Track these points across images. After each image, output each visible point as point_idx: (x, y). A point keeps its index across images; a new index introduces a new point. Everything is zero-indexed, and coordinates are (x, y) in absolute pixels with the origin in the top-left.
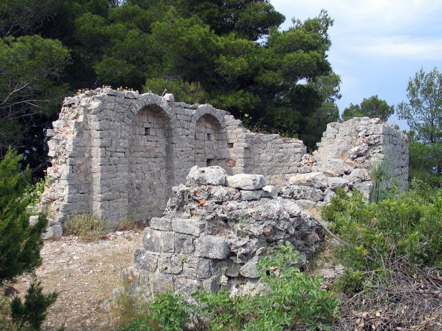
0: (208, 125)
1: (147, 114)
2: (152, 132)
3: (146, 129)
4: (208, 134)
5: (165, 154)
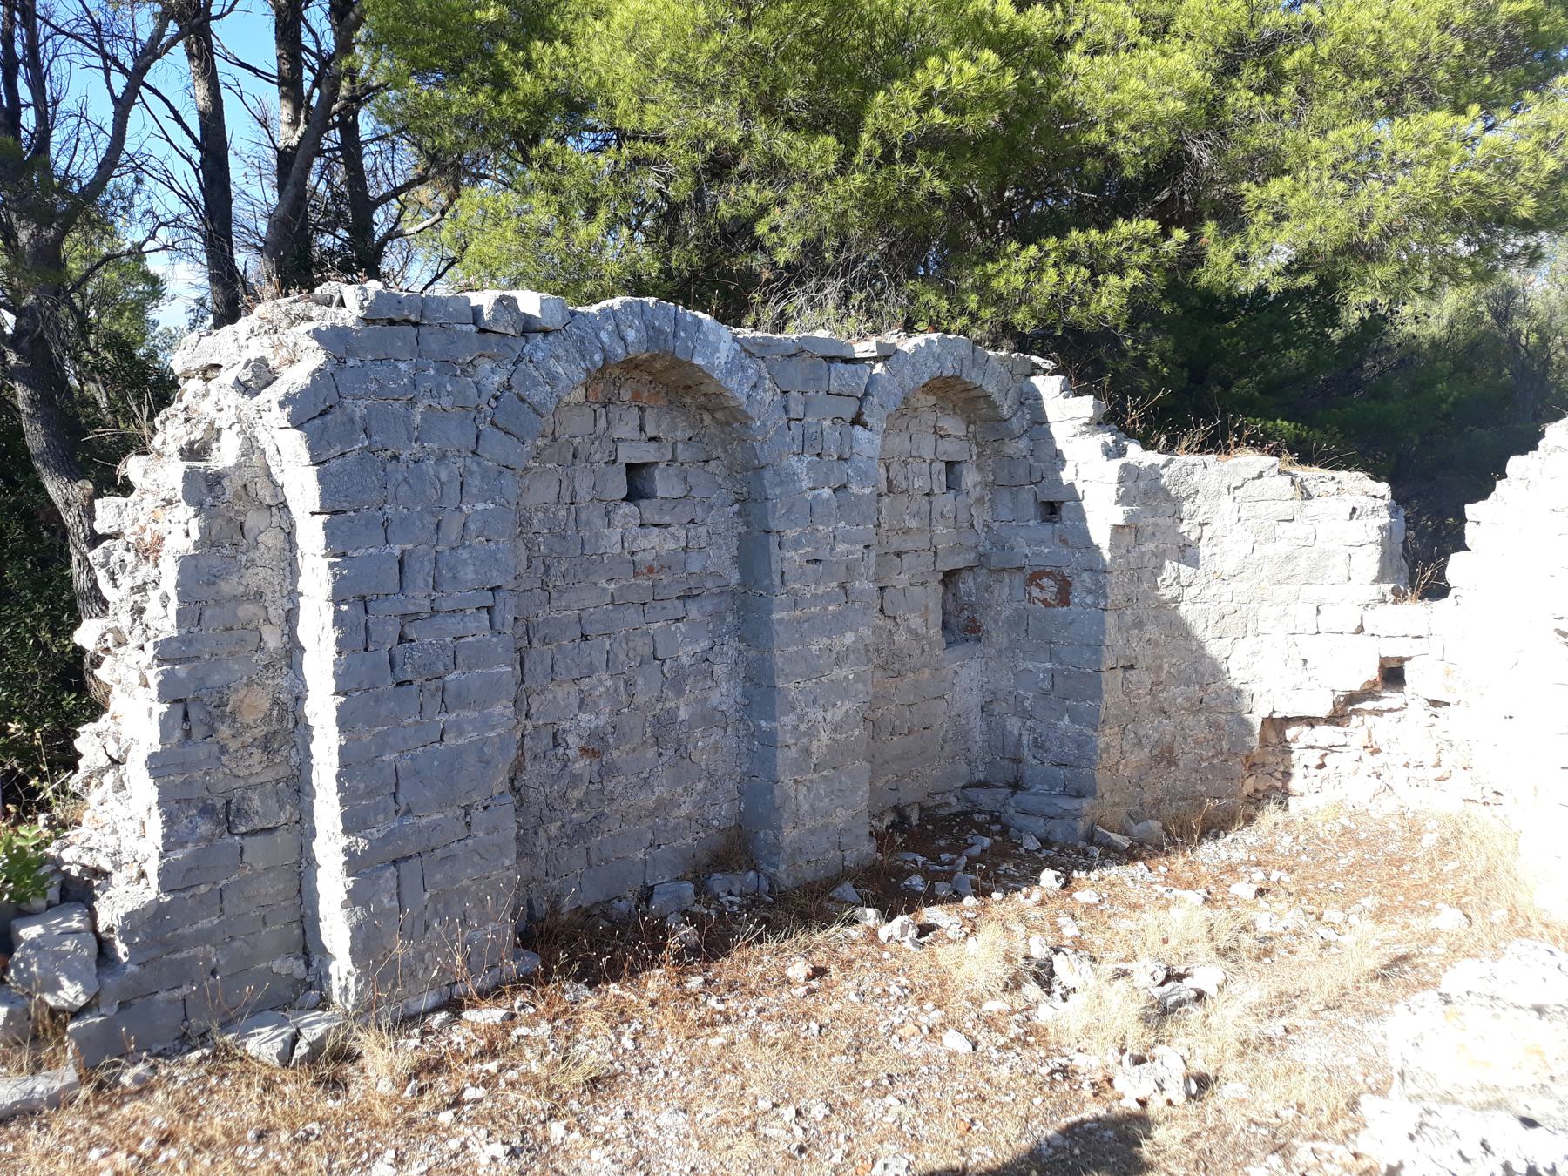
0: (953, 425)
1: (636, 396)
2: (665, 485)
3: (634, 470)
5: (734, 577)
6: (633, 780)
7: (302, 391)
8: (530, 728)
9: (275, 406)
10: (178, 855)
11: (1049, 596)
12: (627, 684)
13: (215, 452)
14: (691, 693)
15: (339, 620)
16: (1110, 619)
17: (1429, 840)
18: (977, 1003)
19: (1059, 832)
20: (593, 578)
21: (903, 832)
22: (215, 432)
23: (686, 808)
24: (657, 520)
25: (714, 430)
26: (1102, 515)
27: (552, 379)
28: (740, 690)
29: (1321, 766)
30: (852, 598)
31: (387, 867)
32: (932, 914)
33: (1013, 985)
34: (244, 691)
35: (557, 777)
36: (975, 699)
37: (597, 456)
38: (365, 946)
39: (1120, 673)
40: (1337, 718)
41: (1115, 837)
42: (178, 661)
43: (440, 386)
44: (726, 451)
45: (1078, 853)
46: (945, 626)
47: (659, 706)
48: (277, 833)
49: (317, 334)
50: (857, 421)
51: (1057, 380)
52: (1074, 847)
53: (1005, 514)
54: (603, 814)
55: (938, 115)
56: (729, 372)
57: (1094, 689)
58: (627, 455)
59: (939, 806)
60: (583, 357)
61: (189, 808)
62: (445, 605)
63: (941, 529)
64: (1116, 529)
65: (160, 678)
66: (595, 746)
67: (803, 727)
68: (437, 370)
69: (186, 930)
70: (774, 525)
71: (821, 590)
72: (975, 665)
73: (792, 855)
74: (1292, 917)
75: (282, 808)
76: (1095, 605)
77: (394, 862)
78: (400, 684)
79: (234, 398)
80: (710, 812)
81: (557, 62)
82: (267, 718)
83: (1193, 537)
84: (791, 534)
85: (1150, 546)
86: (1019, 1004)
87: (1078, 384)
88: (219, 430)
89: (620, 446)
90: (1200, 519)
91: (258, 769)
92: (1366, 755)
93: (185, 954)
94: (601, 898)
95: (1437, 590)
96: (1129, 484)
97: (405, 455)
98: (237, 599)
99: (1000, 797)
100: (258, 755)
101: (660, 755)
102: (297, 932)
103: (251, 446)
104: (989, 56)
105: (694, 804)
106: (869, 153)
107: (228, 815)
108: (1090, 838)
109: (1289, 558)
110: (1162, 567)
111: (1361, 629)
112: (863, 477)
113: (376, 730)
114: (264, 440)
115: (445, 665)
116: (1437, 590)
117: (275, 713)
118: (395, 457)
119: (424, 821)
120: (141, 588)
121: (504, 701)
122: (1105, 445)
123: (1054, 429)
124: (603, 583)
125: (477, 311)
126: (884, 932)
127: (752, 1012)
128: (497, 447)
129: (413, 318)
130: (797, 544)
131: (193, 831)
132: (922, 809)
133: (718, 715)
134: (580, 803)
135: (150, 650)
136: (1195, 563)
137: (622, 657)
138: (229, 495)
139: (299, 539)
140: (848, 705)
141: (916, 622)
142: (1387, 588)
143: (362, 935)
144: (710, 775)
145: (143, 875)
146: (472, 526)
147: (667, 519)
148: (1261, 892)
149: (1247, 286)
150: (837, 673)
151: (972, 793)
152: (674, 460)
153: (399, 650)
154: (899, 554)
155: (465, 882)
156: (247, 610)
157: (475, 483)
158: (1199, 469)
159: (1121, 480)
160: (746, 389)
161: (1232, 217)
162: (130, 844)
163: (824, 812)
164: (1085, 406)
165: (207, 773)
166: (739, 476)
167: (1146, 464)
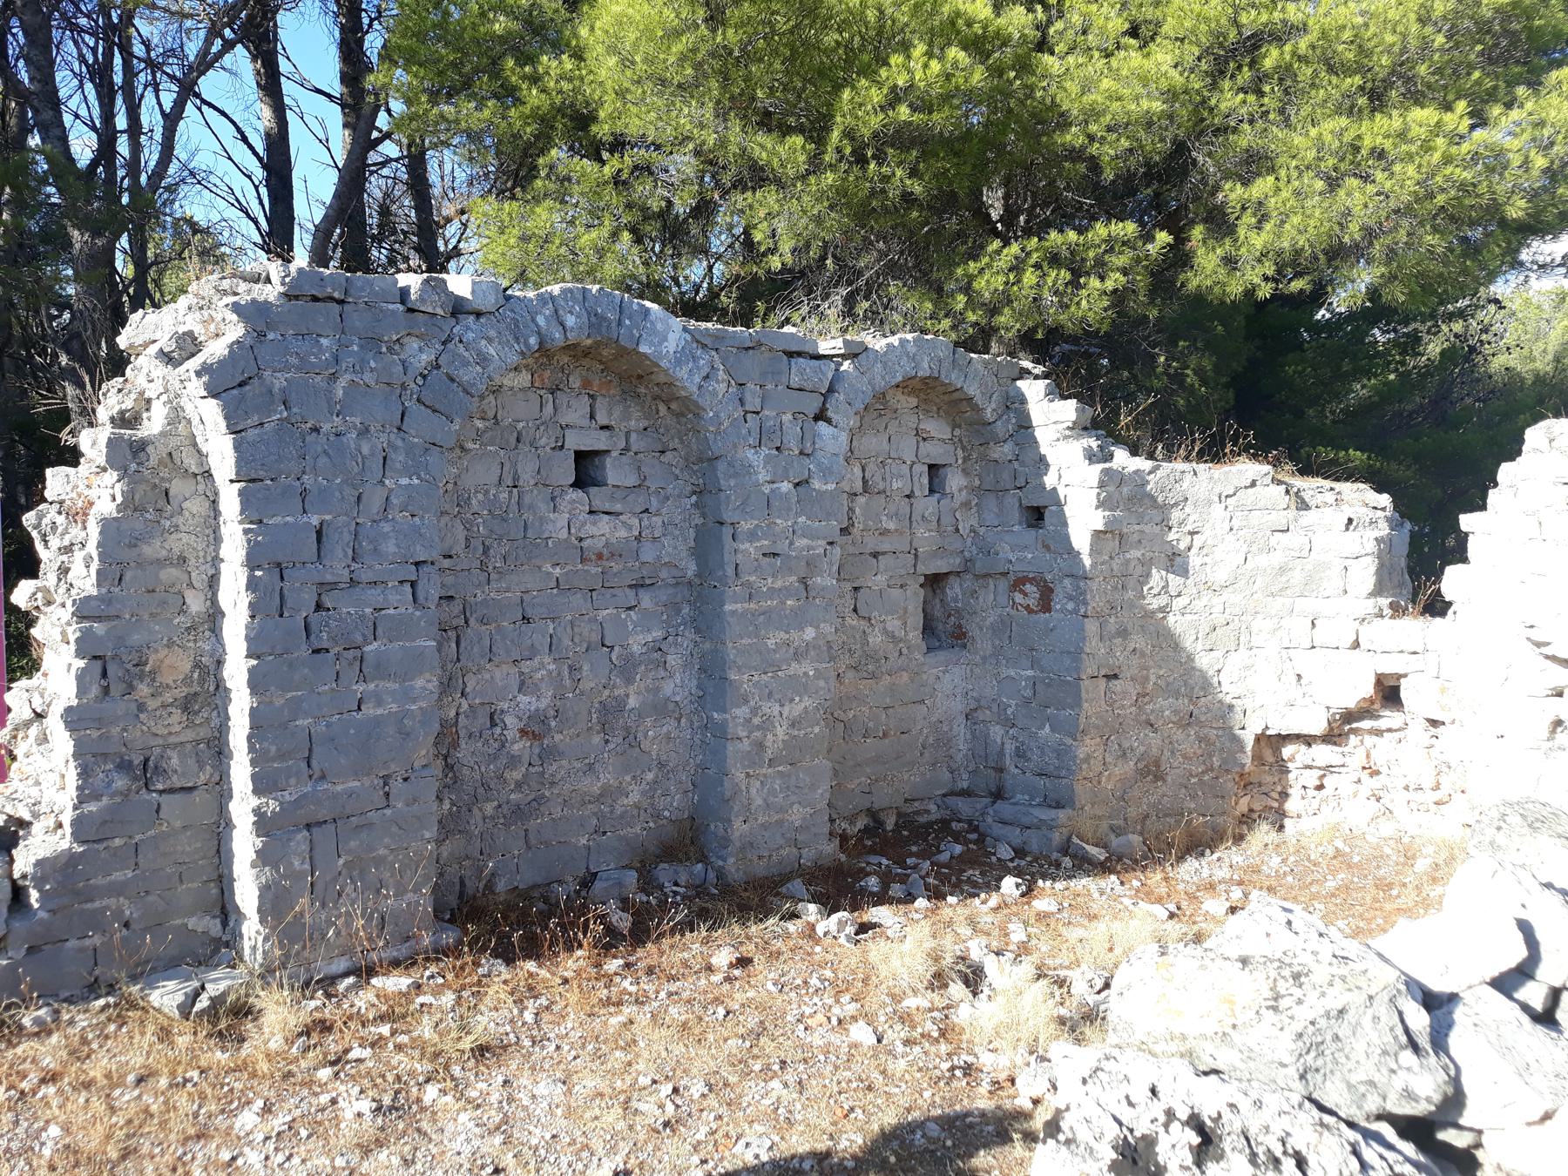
0: (937, 428)
1: (586, 384)
2: (616, 473)
3: (581, 457)
4: (933, 468)
6: (578, 765)
7: (219, 362)
8: (465, 706)
9: (193, 375)
10: (92, 807)
11: (1032, 602)
13: (145, 422)
14: (639, 683)
15: (252, 585)
16: (1091, 626)
17: (1422, 865)
18: (896, 998)
19: (1034, 842)
20: (538, 562)
21: (878, 835)
23: (634, 797)
24: (607, 507)
25: (670, 421)
26: (1083, 519)
27: (483, 360)
28: (695, 682)
29: (1320, 787)
30: (812, 594)
31: (300, 830)
34: (163, 652)
35: (494, 758)
36: (958, 706)
37: (543, 441)
38: (273, 904)
39: (1102, 683)
40: (1334, 736)
41: (1093, 850)
42: (98, 619)
43: (363, 361)
44: (682, 442)
45: (1050, 865)
47: (607, 693)
48: (196, 792)
49: (236, 308)
50: (820, 416)
51: (1042, 384)
52: (1047, 857)
53: (991, 519)
54: (543, 796)
56: (678, 362)
58: (575, 442)
59: (917, 813)
60: (517, 339)
61: (105, 763)
62: (365, 576)
63: (922, 532)
64: (1097, 534)
65: (78, 634)
66: (536, 729)
67: (756, 721)
68: (361, 347)
69: (99, 881)
70: (728, 516)
71: (779, 584)
72: (958, 672)
73: (743, 849)
75: (201, 768)
76: (1076, 611)
77: (308, 826)
78: (316, 651)
79: (160, 370)
80: (661, 803)
82: (187, 680)
83: (1182, 546)
84: (746, 526)
85: (1135, 554)
86: (940, 1002)
88: (149, 401)
89: (568, 432)
90: (1190, 527)
91: (177, 728)
92: (1365, 776)
93: (97, 904)
94: (539, 880)
95: (1437, 607)
96: (1111, 489)
97: (326, 427)
98: (161, 563)
99: (979, 806)
100: (177, 715)
101: (607, 742)
102: (215, 891)
103: (177, 416)
105: (644, 793)
106: (839, 150)
107: (146, 772)
108: (1065, 850)
109: (1283, 570)
110: (1149, 575)
111: (1356, 645)
112: (826, 473)
113: (289, 695)
115: (364, 635)
116: (1437, 607)
117: (196, 675)
118: (316, 430)
119: (339, 788)
120: (68, 550)
121: (428, 676)
123: (1039, 434)
124: (548, 567)
125: (404, 292)
127: (663, 995)
128: (422, 424)
129: (336, 295)
130: (752, 536)
131: (109, 784)
132: (899, 815)
133: (671, 706)
134: (519, 785)
135: (70, 609)
136: (1184, 572)
137: (567, 642)
138: (153, 462)
139: (222, 507)
140: (807, 702)
141: (893, 624)
142: (1384, 602)
143: (270, 895)
144: (661, 765)
145: (60, 826)
146: (395, 501)
147: (618, 507)
149: (1235, 289)
151: (951, 801)
152: (627, 449)
153: (315, 619)
154: (875, 555)
155: (382, 852)
156: (170, 574)
157: (398, 459)
158: (1188, 477)
159: (1102, 485)
160: (697, 379)
163: (778, 806)
164: (1068, 409)
165: (124, 730)
166: (695, 468)
167: (1131, 469)
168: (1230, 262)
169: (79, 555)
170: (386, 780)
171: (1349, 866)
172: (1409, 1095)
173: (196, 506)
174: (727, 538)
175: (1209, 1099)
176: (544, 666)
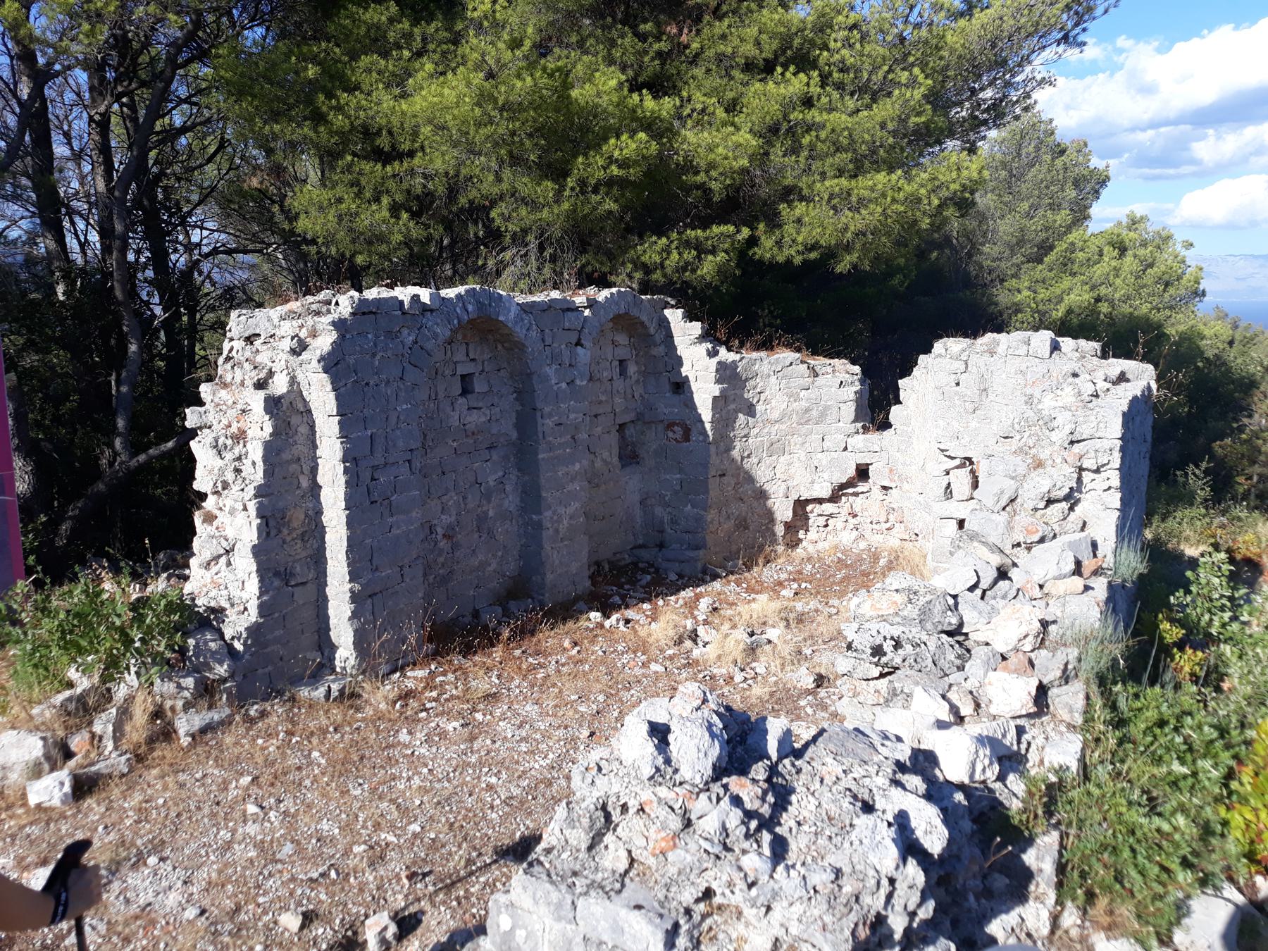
0: (622, 339)
1: (465, 337)
2: (479, 386)
4: (621, 362)
5: (514, 435)
9: (314, 363)
11: (678, 437)
12: (464, 498)
15: (346, 471)
17: (883, 562)
22: (271, 374)
23: (494, 566)
27: (436, 336)
29: (826, 526)
32: (630, 614)
33: (679, 641)
35: (432, 551)
36: (636, 498)
40: (834, 498)
41: (719, 570)
46: (620, 458)
50: (578, 343)
51: (680, 311)
55: (615, 170)
57: (702, 486)
58: (462, 370)
59: (619, 560)
62: (391, 460)
63: (618, 400)
69: (269, 637)
70: (539, 405)
74: (813, 604)
81: (359, 108)
84: (547, 410)
85: (732, 406)
87: (690, 316)
92: (850, 518)
95: (885, 425)
97: (372, 383)
98: (289, 462)
103: (293, 381)
104: (642, 135)
108: (704, 572)
109: (807, 410)
111: (845, 449)
114: (300, 377)
116: (885, 425)
118: (367, 384)
120: (239, 459)
122: (708, 350)
123: (677, 341)
126: (607, 624)
128: (412, 375)
130: (550, 415)
132: (609, 563)
135: (250, 491)
140: (577, 505)
141: (606, 455)
142: (859, 425)
145: (246, 609)
147: (480, 405)
148: (796, 594)
149: (781, 259)
150: (571, 487)
151: (636, 552)
154: (596, 416)
159: (717, 371)
161: (774, 222)
162: (236, 593)
163: (566, 564)
164: (696, 328)
167: (730, 360)
168: (779, 243)
169: (247, 463)
170: (401, 568)
171: (847, 566)
172: (950, 624)
173: (303, 430)
174: (539, 419)
175: (896, 632)
176: (452, 499)
